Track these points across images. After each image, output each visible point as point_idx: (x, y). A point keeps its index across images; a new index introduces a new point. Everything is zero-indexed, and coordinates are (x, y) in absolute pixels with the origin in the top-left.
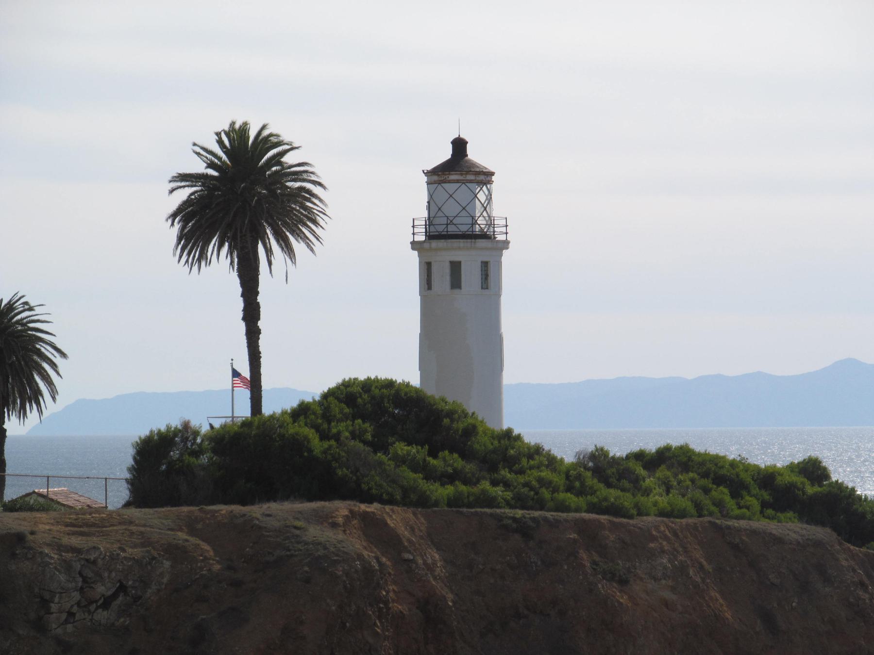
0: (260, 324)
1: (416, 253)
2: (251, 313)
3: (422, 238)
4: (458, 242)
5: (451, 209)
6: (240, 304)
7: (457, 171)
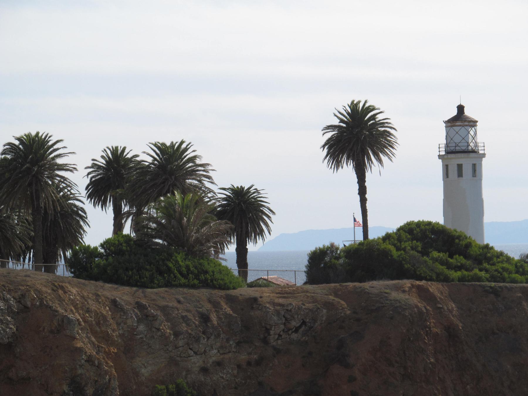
0: (367, 196)
2: (362, 191)
3: (444, 153)
4: (461, 155)
5: (457, 139)
6: (357, 187)
7: (460, 120)
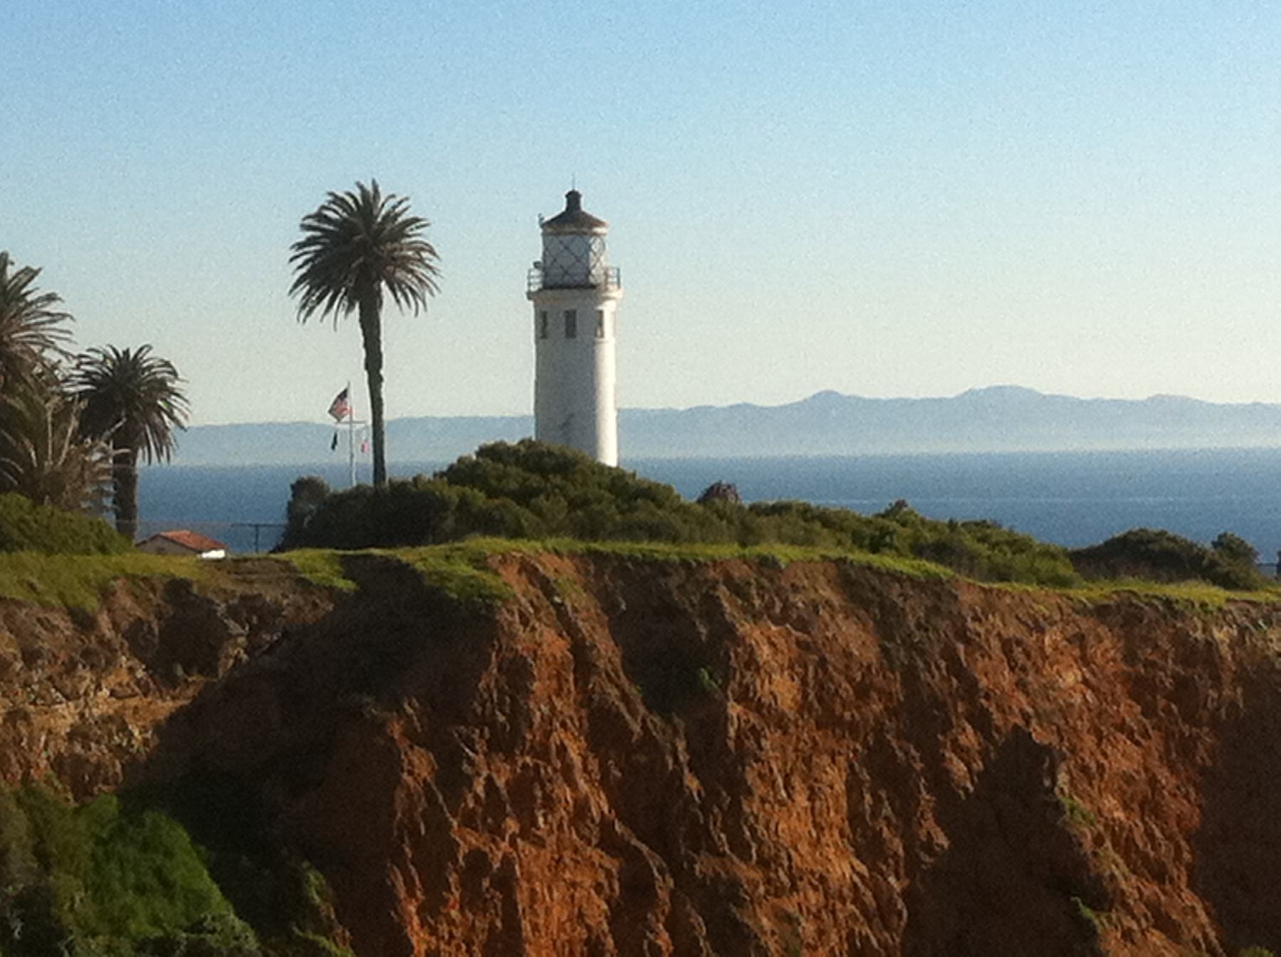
1: (531, 303)
2: (373, 362)
4: (567, 292)
5: (566, 261)
7: (571, 224)
